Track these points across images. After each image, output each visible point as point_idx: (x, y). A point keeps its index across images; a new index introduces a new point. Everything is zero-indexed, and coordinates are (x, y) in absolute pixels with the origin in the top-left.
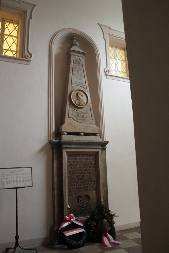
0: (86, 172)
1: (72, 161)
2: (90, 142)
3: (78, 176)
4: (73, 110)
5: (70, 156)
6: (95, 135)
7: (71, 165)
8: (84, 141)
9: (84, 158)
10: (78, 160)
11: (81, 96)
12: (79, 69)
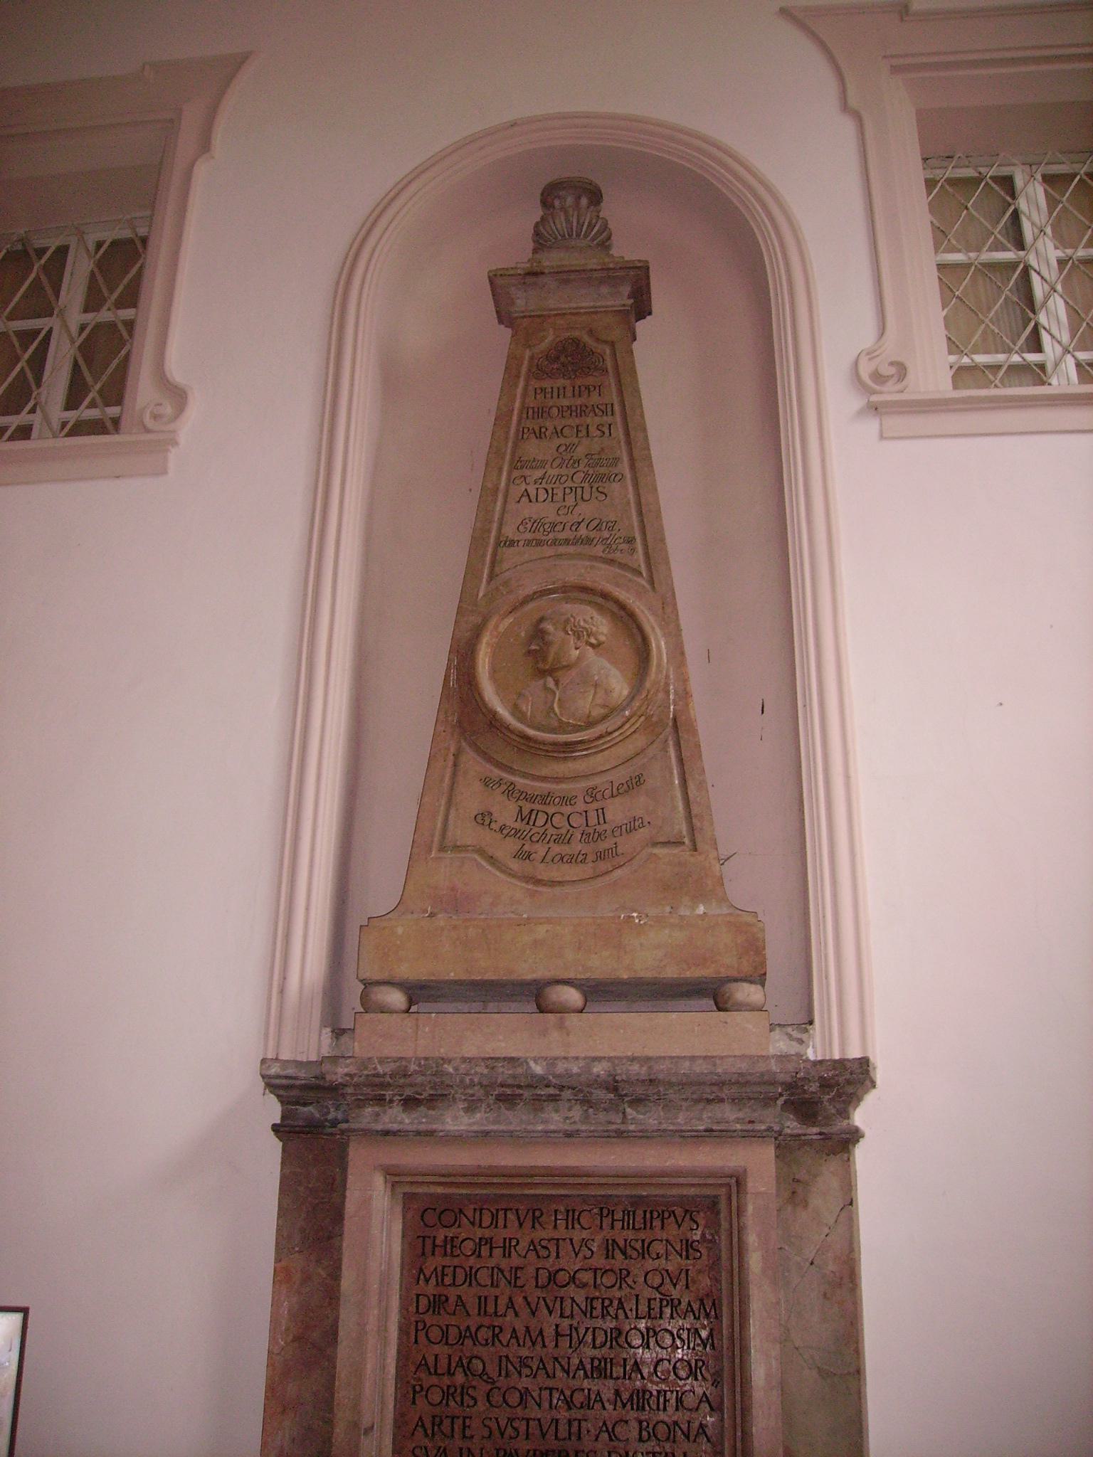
0: (606, 1389)
1: (447, 1261)
2: (635, 1067)
3: (511, 1420)
4: (496, 773)
5: (431, 1218)
6: (715, 993)
7: (437, 1303)
8: (561, 1067)
9: (584, 1242)
10: (516, 1261)
11: (572, 640)
12: (582, 411)
